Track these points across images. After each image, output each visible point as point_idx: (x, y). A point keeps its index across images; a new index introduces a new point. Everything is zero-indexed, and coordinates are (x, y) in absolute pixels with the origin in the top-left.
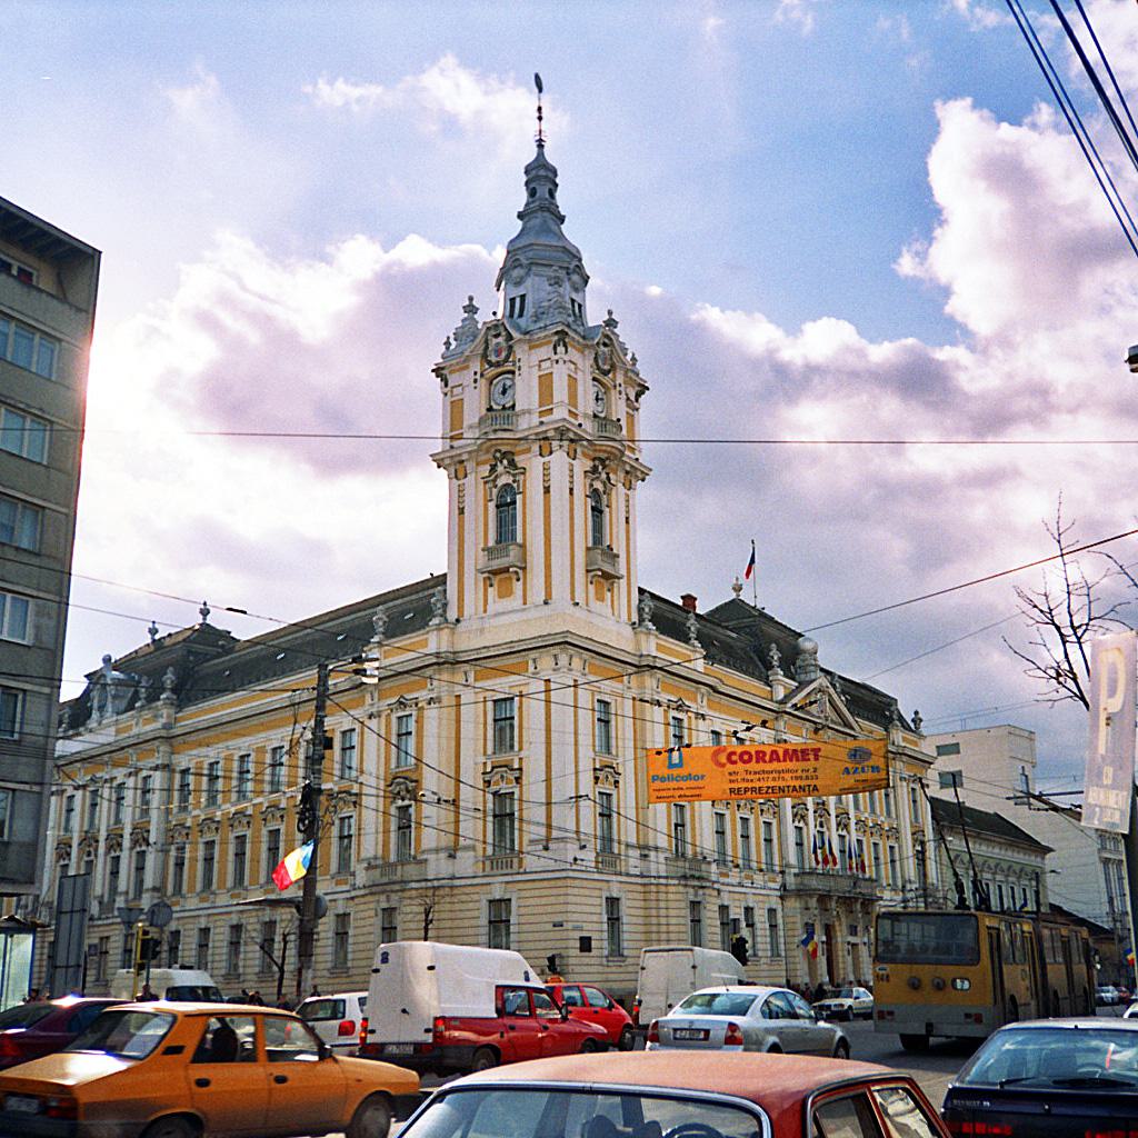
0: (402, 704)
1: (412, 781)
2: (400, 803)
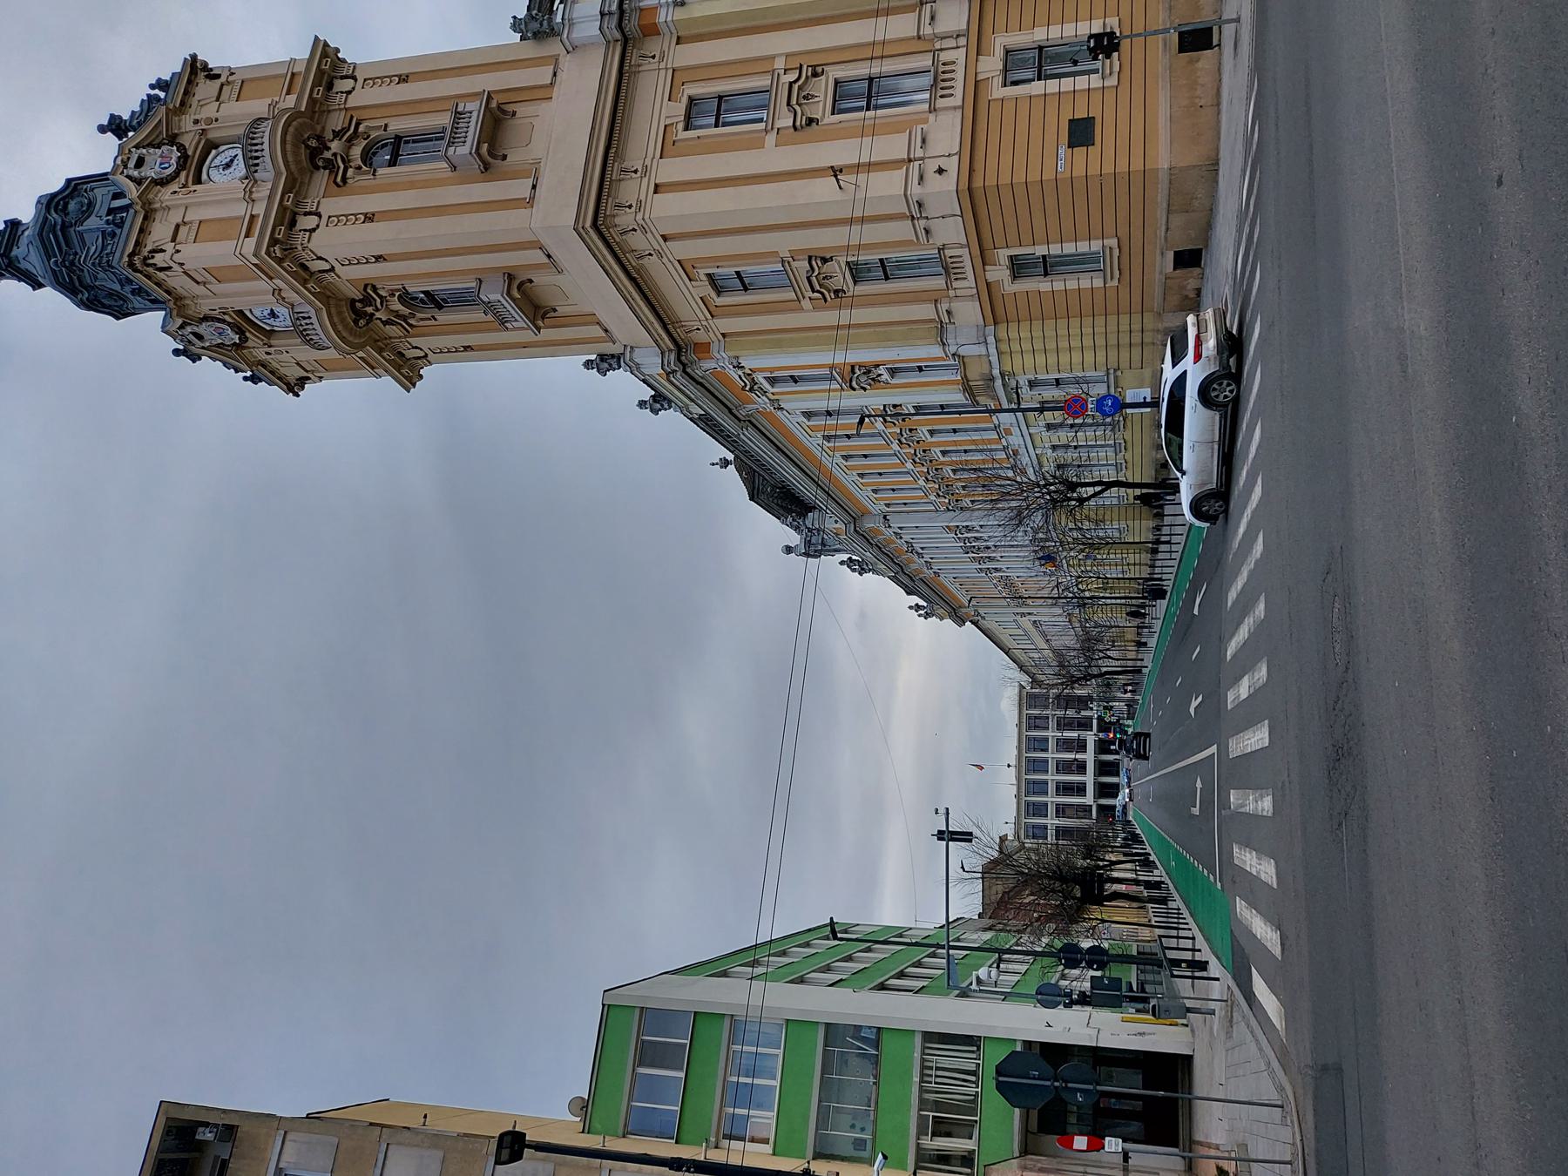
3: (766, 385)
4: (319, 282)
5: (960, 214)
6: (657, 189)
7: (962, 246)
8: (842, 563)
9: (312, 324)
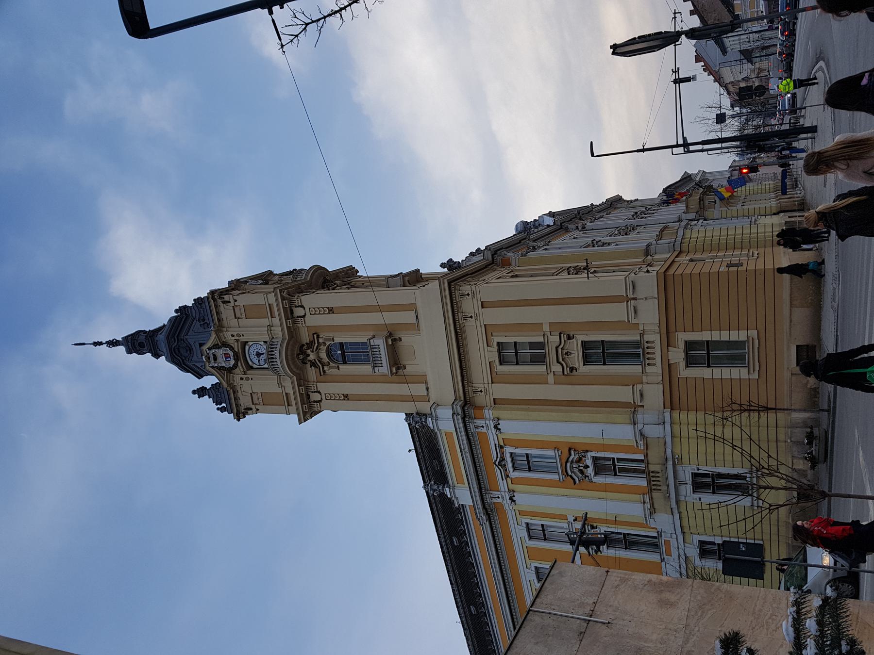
0: (501, 463)
1: (570, 455)
2: (590, 471)
4: (295, 322)
5: (656, 296)
7: (655, 333)
9: (276, 362)
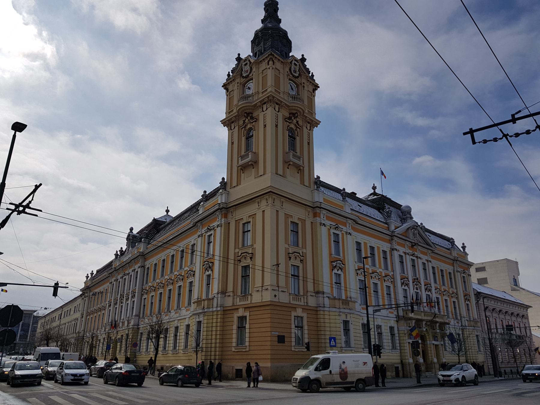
3: (209, 234)
6: (277, 211)
7: (251, 301)
8: (122, 248)
